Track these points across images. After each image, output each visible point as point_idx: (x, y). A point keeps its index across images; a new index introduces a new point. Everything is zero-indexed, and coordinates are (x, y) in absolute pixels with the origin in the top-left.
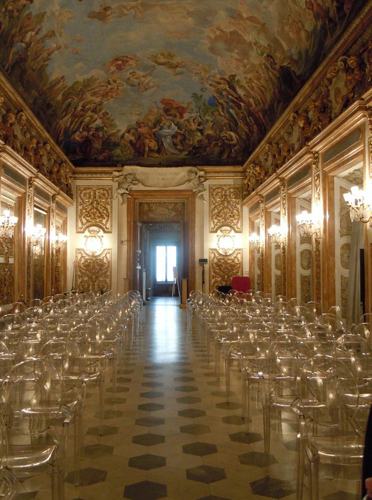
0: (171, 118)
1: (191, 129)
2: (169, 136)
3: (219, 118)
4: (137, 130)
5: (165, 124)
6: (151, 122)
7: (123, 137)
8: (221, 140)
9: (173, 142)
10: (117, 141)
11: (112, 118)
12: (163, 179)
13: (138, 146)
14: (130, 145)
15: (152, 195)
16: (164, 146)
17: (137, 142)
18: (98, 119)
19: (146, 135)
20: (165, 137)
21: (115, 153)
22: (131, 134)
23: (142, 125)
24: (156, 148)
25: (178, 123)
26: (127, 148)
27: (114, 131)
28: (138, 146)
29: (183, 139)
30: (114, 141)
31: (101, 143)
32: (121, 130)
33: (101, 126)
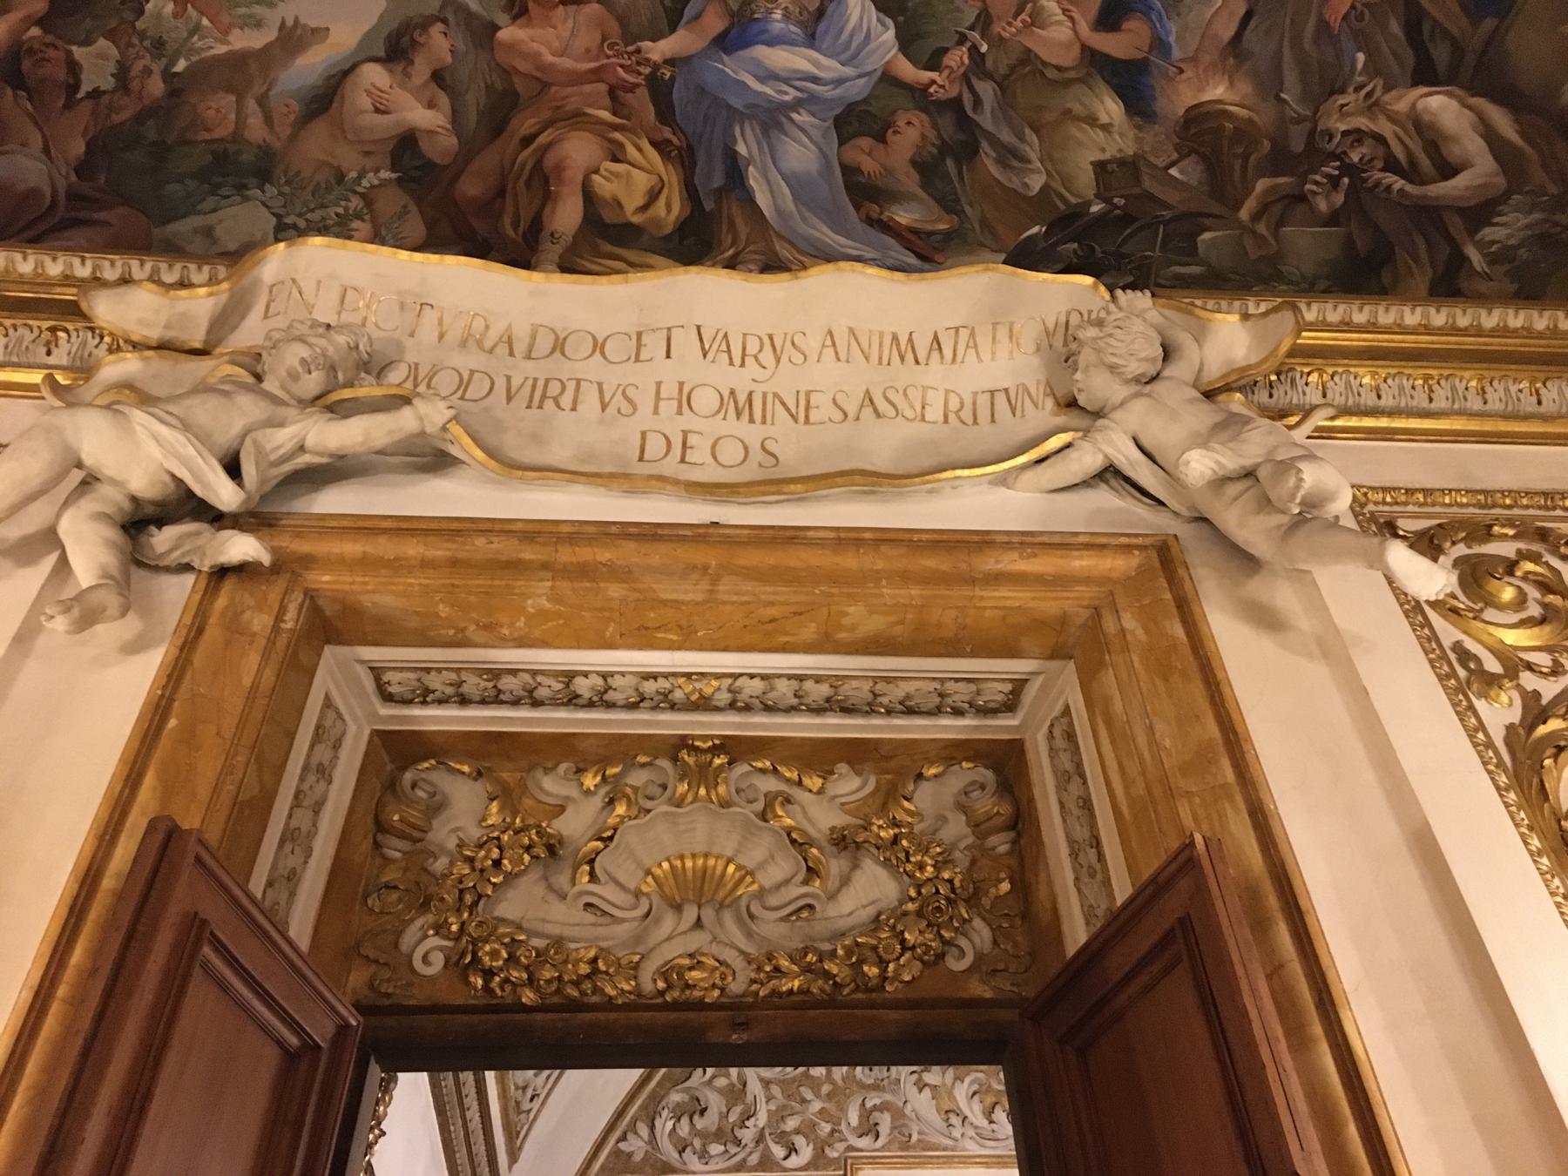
1: (1028, 57)
2: (801, 117)
8: (1331, 169)
9: (849, 171)
10: (256, 128)
12: (741, 406)
14: (385, 174)
16: (751, 201)
17: (467, 154)
19: (573, 97)
20: (772, 119)
24: (670, 211)
26: (356, 203)
27: (244, 40)
28: (471, 187)
29: (945, 149)
31: (78, 148)
32: (320, 33)
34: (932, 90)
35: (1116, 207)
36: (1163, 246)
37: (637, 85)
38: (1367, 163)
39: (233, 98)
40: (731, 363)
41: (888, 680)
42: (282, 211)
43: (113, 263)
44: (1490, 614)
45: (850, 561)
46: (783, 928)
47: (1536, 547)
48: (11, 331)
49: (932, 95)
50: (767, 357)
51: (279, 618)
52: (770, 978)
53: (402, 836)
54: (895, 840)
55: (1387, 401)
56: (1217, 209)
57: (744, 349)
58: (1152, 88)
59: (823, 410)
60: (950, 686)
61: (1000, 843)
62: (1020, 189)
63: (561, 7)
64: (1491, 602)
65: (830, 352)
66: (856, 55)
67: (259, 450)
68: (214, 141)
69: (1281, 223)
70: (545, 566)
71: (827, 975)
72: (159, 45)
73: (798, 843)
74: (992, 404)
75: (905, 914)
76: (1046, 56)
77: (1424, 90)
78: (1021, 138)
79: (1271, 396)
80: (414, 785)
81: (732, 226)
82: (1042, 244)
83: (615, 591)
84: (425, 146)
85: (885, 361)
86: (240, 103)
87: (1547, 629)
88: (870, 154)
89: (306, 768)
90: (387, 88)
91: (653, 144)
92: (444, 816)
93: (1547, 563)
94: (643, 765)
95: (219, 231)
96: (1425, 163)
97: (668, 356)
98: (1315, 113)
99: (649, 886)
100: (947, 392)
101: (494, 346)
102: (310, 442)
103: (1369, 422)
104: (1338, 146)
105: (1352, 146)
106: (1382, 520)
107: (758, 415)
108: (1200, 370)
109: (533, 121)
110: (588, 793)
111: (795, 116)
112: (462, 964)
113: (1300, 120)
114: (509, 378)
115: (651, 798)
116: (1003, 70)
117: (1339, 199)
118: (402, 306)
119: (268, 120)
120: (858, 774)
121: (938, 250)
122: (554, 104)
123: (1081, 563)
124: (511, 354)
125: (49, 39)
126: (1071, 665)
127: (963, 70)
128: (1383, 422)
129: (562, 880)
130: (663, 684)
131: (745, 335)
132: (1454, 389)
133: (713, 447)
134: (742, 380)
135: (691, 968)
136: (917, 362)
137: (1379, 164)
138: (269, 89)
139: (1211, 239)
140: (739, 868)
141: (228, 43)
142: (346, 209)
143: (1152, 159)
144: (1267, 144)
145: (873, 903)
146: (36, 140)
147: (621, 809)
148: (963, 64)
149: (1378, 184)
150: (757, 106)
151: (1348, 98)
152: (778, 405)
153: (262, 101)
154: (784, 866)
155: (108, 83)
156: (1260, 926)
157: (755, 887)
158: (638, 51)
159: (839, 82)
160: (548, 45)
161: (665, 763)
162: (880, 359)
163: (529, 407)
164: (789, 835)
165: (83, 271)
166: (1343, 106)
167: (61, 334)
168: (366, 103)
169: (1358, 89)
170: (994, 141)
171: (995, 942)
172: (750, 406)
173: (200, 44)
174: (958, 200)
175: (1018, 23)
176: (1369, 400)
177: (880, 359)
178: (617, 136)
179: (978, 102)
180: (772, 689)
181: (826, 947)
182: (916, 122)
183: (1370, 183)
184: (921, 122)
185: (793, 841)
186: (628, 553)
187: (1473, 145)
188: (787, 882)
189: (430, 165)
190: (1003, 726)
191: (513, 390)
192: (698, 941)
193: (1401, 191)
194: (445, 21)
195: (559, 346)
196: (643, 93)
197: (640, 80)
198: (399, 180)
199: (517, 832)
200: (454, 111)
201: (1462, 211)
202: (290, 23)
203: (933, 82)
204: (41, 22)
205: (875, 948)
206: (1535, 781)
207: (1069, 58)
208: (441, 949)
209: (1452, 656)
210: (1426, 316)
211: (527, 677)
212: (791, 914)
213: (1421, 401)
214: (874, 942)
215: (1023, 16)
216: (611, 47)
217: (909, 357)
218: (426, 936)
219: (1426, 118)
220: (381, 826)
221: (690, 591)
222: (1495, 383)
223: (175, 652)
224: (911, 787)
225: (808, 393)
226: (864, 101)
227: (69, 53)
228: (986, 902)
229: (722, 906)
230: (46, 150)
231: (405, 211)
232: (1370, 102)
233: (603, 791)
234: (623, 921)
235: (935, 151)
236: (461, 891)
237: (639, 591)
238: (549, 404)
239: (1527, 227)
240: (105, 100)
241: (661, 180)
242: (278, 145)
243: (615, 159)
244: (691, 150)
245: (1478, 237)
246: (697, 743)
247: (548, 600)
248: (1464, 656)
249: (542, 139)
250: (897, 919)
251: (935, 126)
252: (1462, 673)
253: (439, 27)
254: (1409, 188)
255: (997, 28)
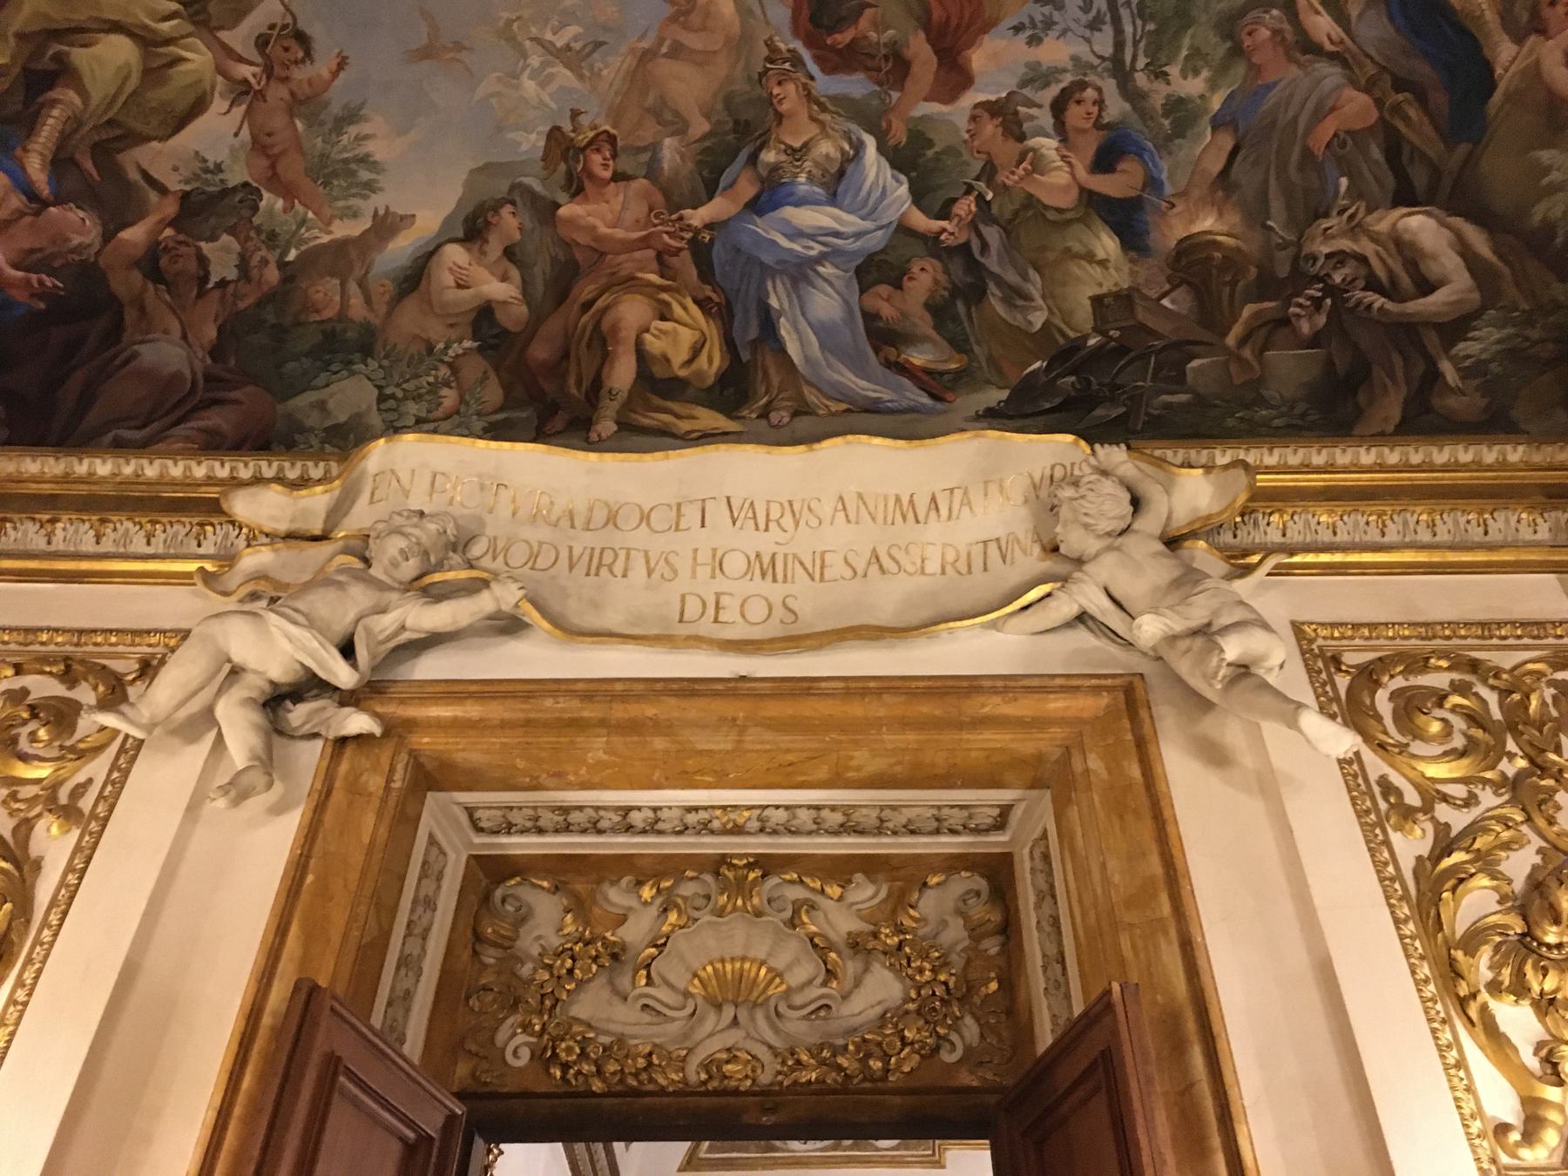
0: (855, 85)
1: (1030, 201)
2: (826, 270)
3: (1287, 76)
4: (546, 211)
5: (798, 154)
6: (679, 126)
7: (415, 277)
9: (870, 317)
11: (338, 98)
12: (767, 568)
13: (540, 352)
14: (467, 344)
15: (633, 727)
16: (782, 351)
17: (537, 320)
18: (219, 104)
19: (626, 264)
20: (800, 273)
21: (322, 406)
22: (495, 248)
23: (597, 159)
24: (712, 363)
25: (919, 138)
26: (444, 371)
27: (343, 230)
28: (540, 352)
29: (955, 292)
30: (328, 313)
31: (211, 333)
32: (408, 220)
33: (237, 175)
34: (943, 237)
35: (1111, 339)
36: (1155, 375)
37: (680, 249)
38: (1350, 283)
39: (338, 282)
40: (757, 529)
41: (893, 808)
42: (383, 383)
43: (246, 465)
44: (1417, 747)
45: (856, 709)
46: (803, 1027)
47: (1468, 678)
48: (168, 527)
49: (943, 242)
50: (788, 521)
51: (389, 780)
52: (792, 1070)
53: (495, 945)
54: (900, 946)
55: (1342, 537)
56: (1206, 336)
57: (768, 515)
58: (1146, 224)
59: (836, 568)
60: (946, 811)
61: (992, 946)
62: (1023, 326)
63: (612, 184)
64: (1419, 735)
65: (841, 515)
66: (874, 209)
67: (368, 632)
68: (323, 321)
69: (1265, 347)
70: (603, 723)
71: (840, 1068)
72: (272, 236)
73: (819, 946)
74: (985, 553)
75: (907, 1012)
76: (1046, 201)
77: (1405, 210)
78: (1026, 278)
79: (1235, 536)
80: (503, 901)
81: (766, 373)
82: (1044, 379)
83: (659, 743)
84: (500, 316)
85: (890, 522)
86: (343, 285)
87: (1465, 762)
88: (888, 300)
89: (415, 902)
90: (466, 266)
91: (696, 302)
92: (531, 923)
93: (1476, 694)
94: (692, 879)
95: (331, 405)
96: (1405, 281)
97: (703, 526)
98: (1299, 239)
99: (696, 988)
100: (945, 545)
101: (558, 520)
102: (408, 624)
103: (1325, 558)
104: (1322, 267)
105: (1335, 268)
106: (1329, 654)
107: (780, 576)
108: (1169, 518)
109: (592, 287)
110: (646, 903)
111: (820, 269)
112: (544, 1058)
113: (1284, 246)
114: (571, 549)
115: (697, 909)
116: (1007, 215)
117: (1321, 320)
118: (482, 487)
119: (368, 300)
120: (873, 882)
121: (951, 390)
122: (609, 271)
123: (1057, 705)
124: (573, 526)
125: (181, 237)
126: (1048, 794)
127: (970, 217)
128: (1338, 558)
129: (624, 982)
130: (703, 815)
131: (768, 502)
132: (1405, 523)
133: (742, 606)
134: (766, 543)
135: (728, 1062)
136: (918, 522)
137: (1361, 283)
138: (367, 272)
139: (1199, 367)
140: (770, 970)
141: (330, 233)
142: (436, 377)
143: (1145, 291)
144: (1253, 271)
145: (879, 1003)
146: (175, 327)
147: (673, 917)
148: (970, 211)
149: (1359, 303)
150: (785, 262)
151: (1333, 221)
152: (797, 565)
153: (361, 284)
154: (806, 969)
155: (232, 274)
156: (1178, 1047)
157: (784, 987)
158: (681, 218)
159: (858, 235)
160: (603, 220)
161: (708, 878)
162: (885, 518)
163: (588, 574)
164: (812, 940)
165: (223, 472)
166: (1326, 229)
167: (209, 528)
168: (449, 279)
169: (1341, 213)
170: (1000, 282)
171: (982, 1036)
172: (774, 569)
173: (306, 235)
174: (967, 340)
175: (1020, 171)
176: (1325, 536)
177: (885, 518)
178: (665, 296)
179: (985, 247)
180: (795, 817)
181: (840, 1042)
182: (928, 267)
183: (1351, 304)
184: (932, 265)
185: (815, 946)
186: (668, 709)
187: (1450, 263)
188: (809, 982)
189: (506, 332)
190: (997, 841)
191: (575, 559)
192: (733, 1037)
193: (1381, 308)
194: (513, 203)
195: (612, 519)
196: (686, 255)
197: (683, 244)
198: (480, 350)
199: (587, 944)
200: (524, 282)
201: (1438, 327)
202: (381, 212)
203: (944, 230)
204: (173, 223)
205: (879, 1044)
206: (1433, 912)
207: (1067, 200)
208: (526, 1044)
209: (1377, 790)
210: (1380, 455)
211: (591, 812)
212: (812, 1013)
213: (1373, 535)
214: (880, 1039)
215: (1024, 165)
216: (656, 216)
217: (910, 516)
218: (514, 1034)
219: (1407, 237)
220: (478, 937)
221: (721, 742)
222: (1445, 516)
223: (310, 814)
224: (916, 896)
225: (823, 554)
226: (882, 251)
227: (199, 249)
228: (977, 1000)
229: (755, 1005)
230: (184, 337)
231: (485, 377)
232: (1353, 224)
233: (659, 901)
234: (673, 1020)
235: (946, 293)
236: (543, 996)
237: (679, 743)
238: (604, 572)
239: (1499, 342)
240: (231, 288)
241: (703, 333)
242: (377, 322)
243: (663, 318)
244: (729, 305)
245: (1453, 352)
246: (735, 861)
247: (605, 753)
248: (1387, 788)
249: (600, 303)
250: (900, 1018)
251: (946, 272)
252: (1383, 806)
253: (508, 208)
254: (1390, 306)
255: (1001, 177)
